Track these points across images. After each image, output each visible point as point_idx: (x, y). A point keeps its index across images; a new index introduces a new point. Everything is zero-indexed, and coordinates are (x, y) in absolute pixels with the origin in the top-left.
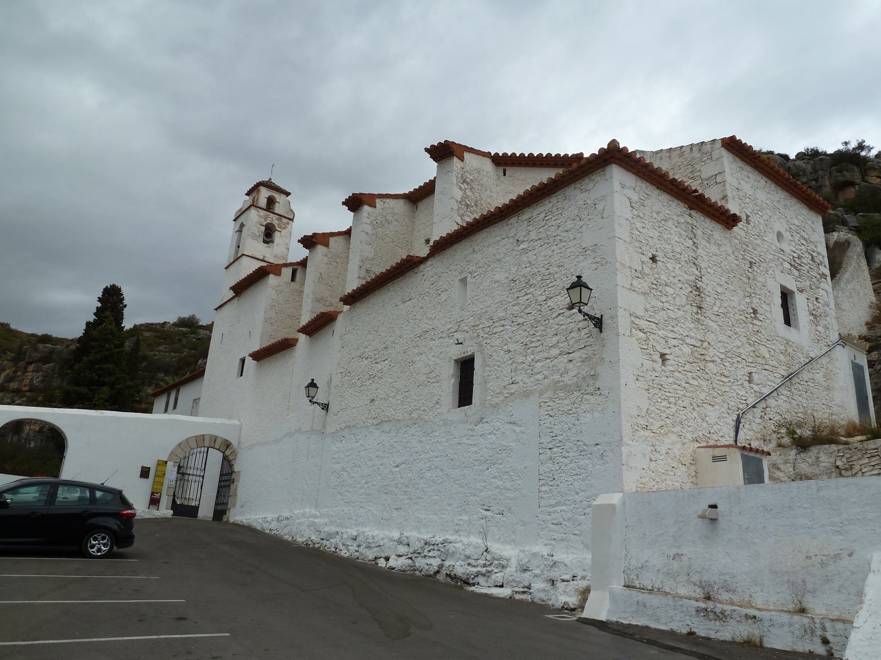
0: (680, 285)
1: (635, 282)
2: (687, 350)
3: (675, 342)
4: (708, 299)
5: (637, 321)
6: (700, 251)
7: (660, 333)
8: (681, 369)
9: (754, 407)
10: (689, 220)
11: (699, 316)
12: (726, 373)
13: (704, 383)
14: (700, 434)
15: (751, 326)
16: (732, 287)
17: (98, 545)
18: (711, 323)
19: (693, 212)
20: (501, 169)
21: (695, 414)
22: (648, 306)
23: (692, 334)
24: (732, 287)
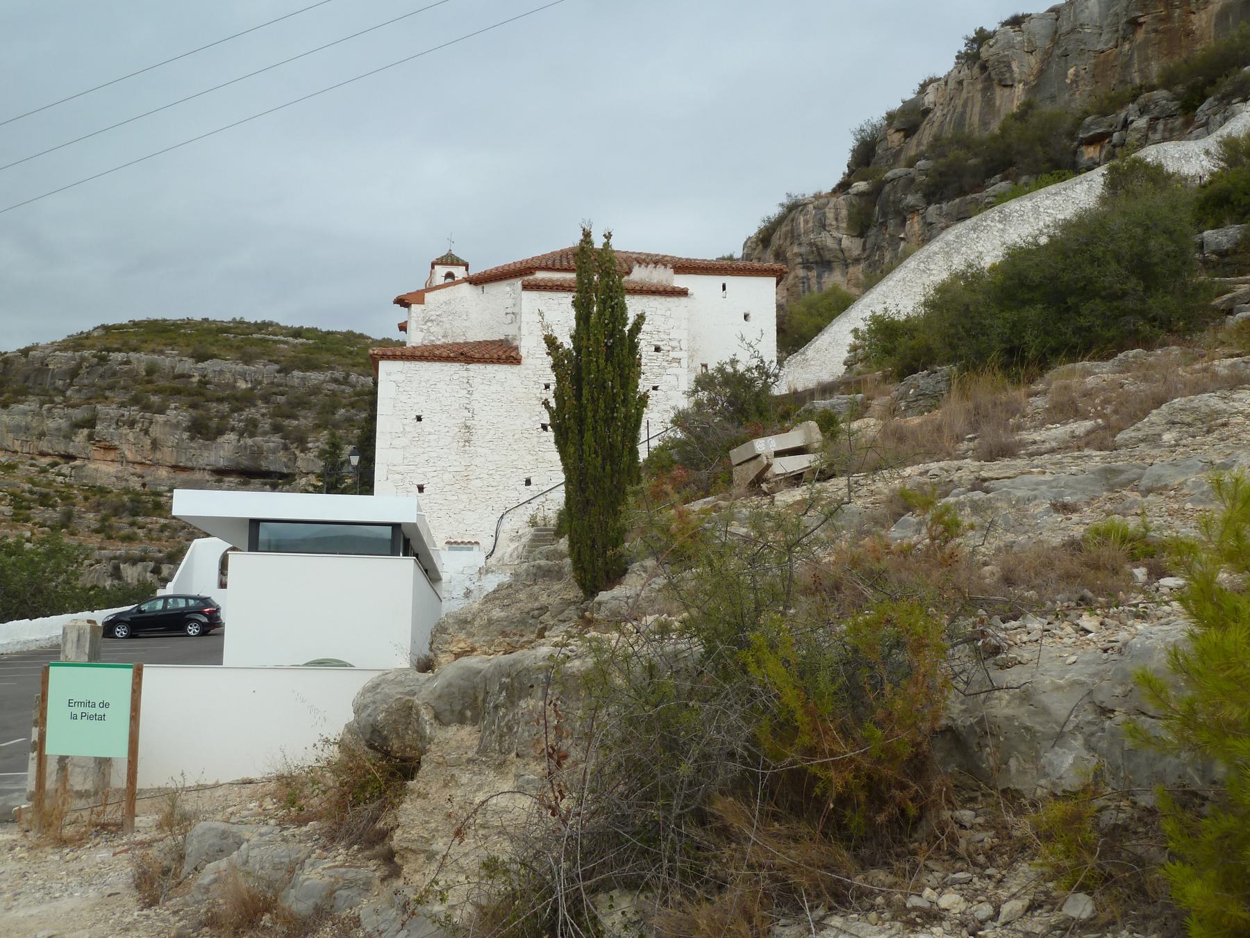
0: (446, 429)
1: (396, 442)
2: (447, 476)
3: (435, 474)
4: (480, 431)
5: (395, 468)
6: (476, 396)
7: (419, 471)
8: (438, 492)
9: (529, 502)
10: (465, 374)
11: (467, 448)
12: (493, 484)
13: (464, 497)
14: (455, 533)
15: (536, 439)
16: (513, 414)
17: (193, 630)
18: (479, 450)
19: (471, 366)
20: (480, 287)
21: (451, 520)
22: (407, 455)
23: (455, 463)
24: (513, 414)
